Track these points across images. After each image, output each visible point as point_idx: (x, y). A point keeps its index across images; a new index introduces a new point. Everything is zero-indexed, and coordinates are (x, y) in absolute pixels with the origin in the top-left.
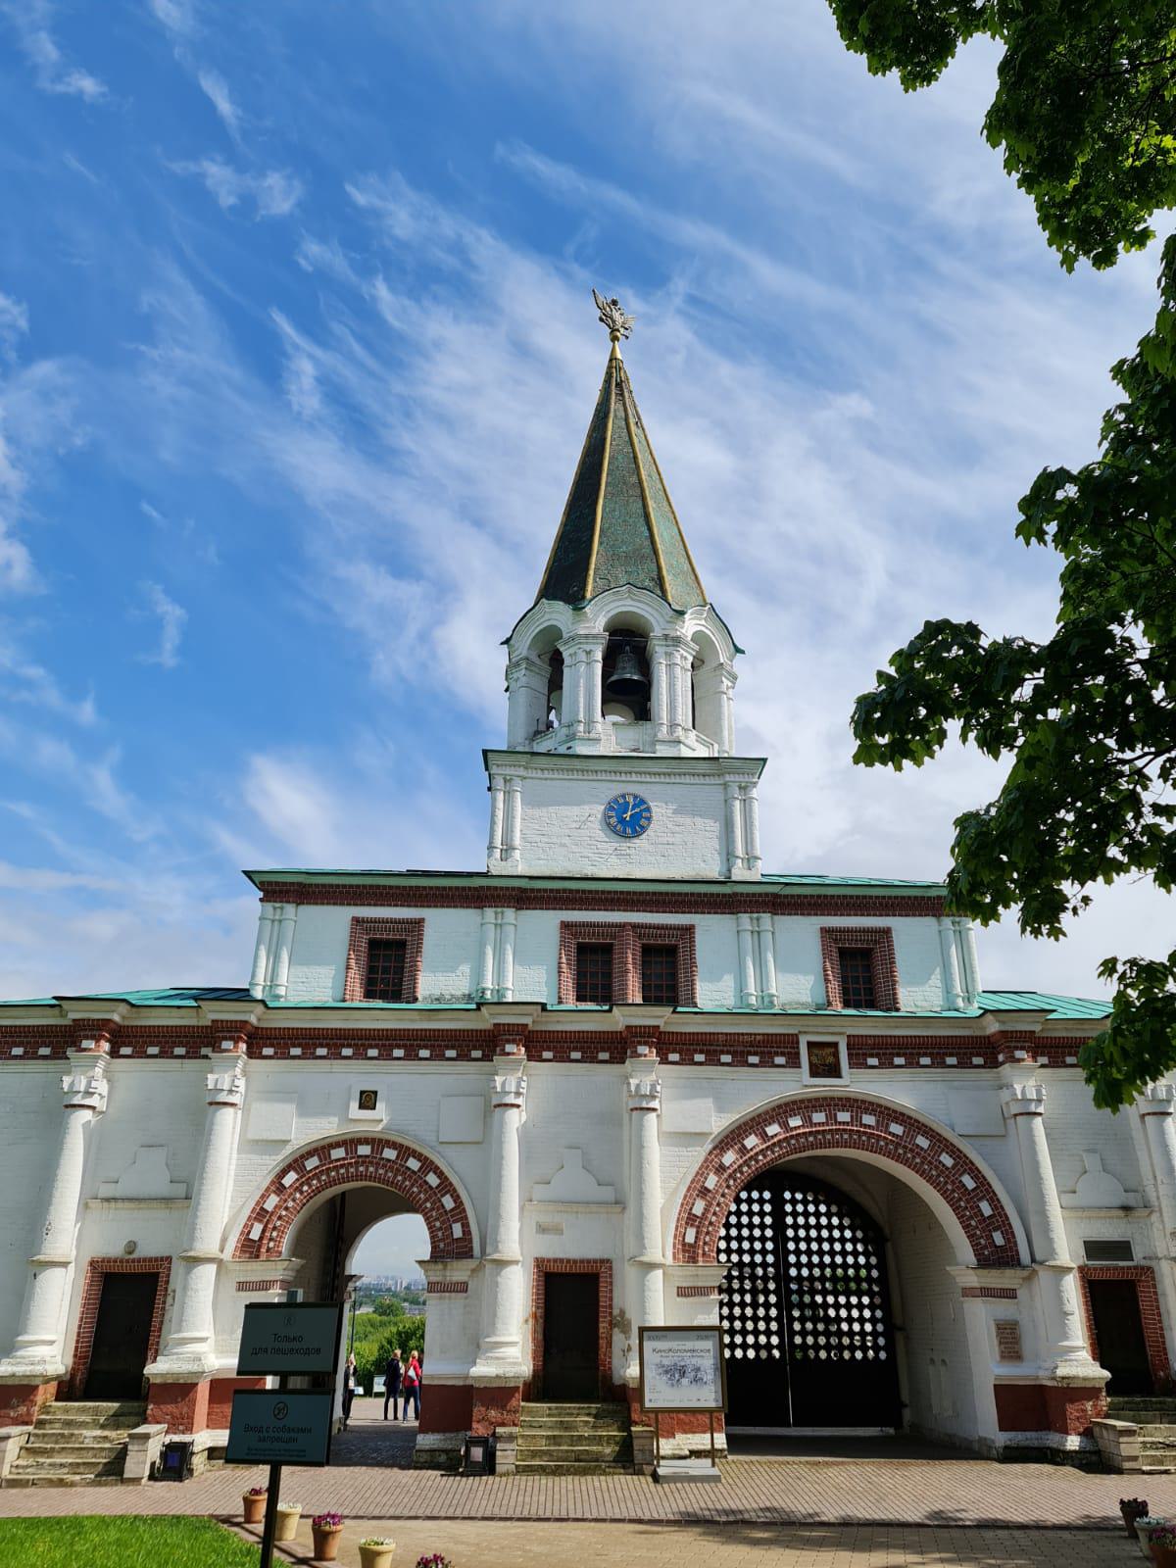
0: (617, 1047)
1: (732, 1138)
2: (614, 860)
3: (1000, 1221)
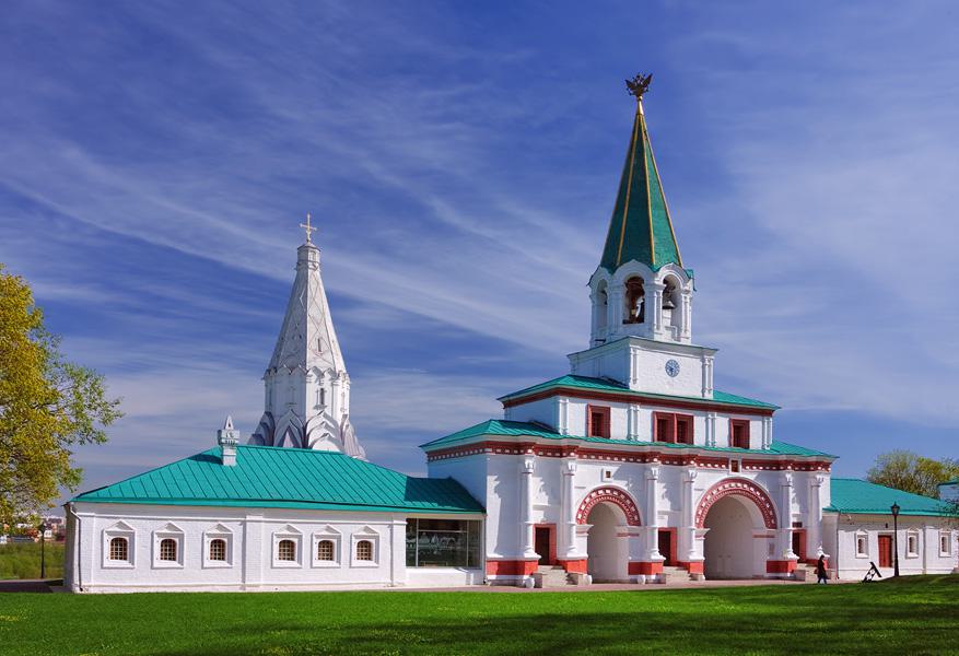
0: (680, 460)
1: (710, 492)
2: (667, 387)
3: (774, 517)
